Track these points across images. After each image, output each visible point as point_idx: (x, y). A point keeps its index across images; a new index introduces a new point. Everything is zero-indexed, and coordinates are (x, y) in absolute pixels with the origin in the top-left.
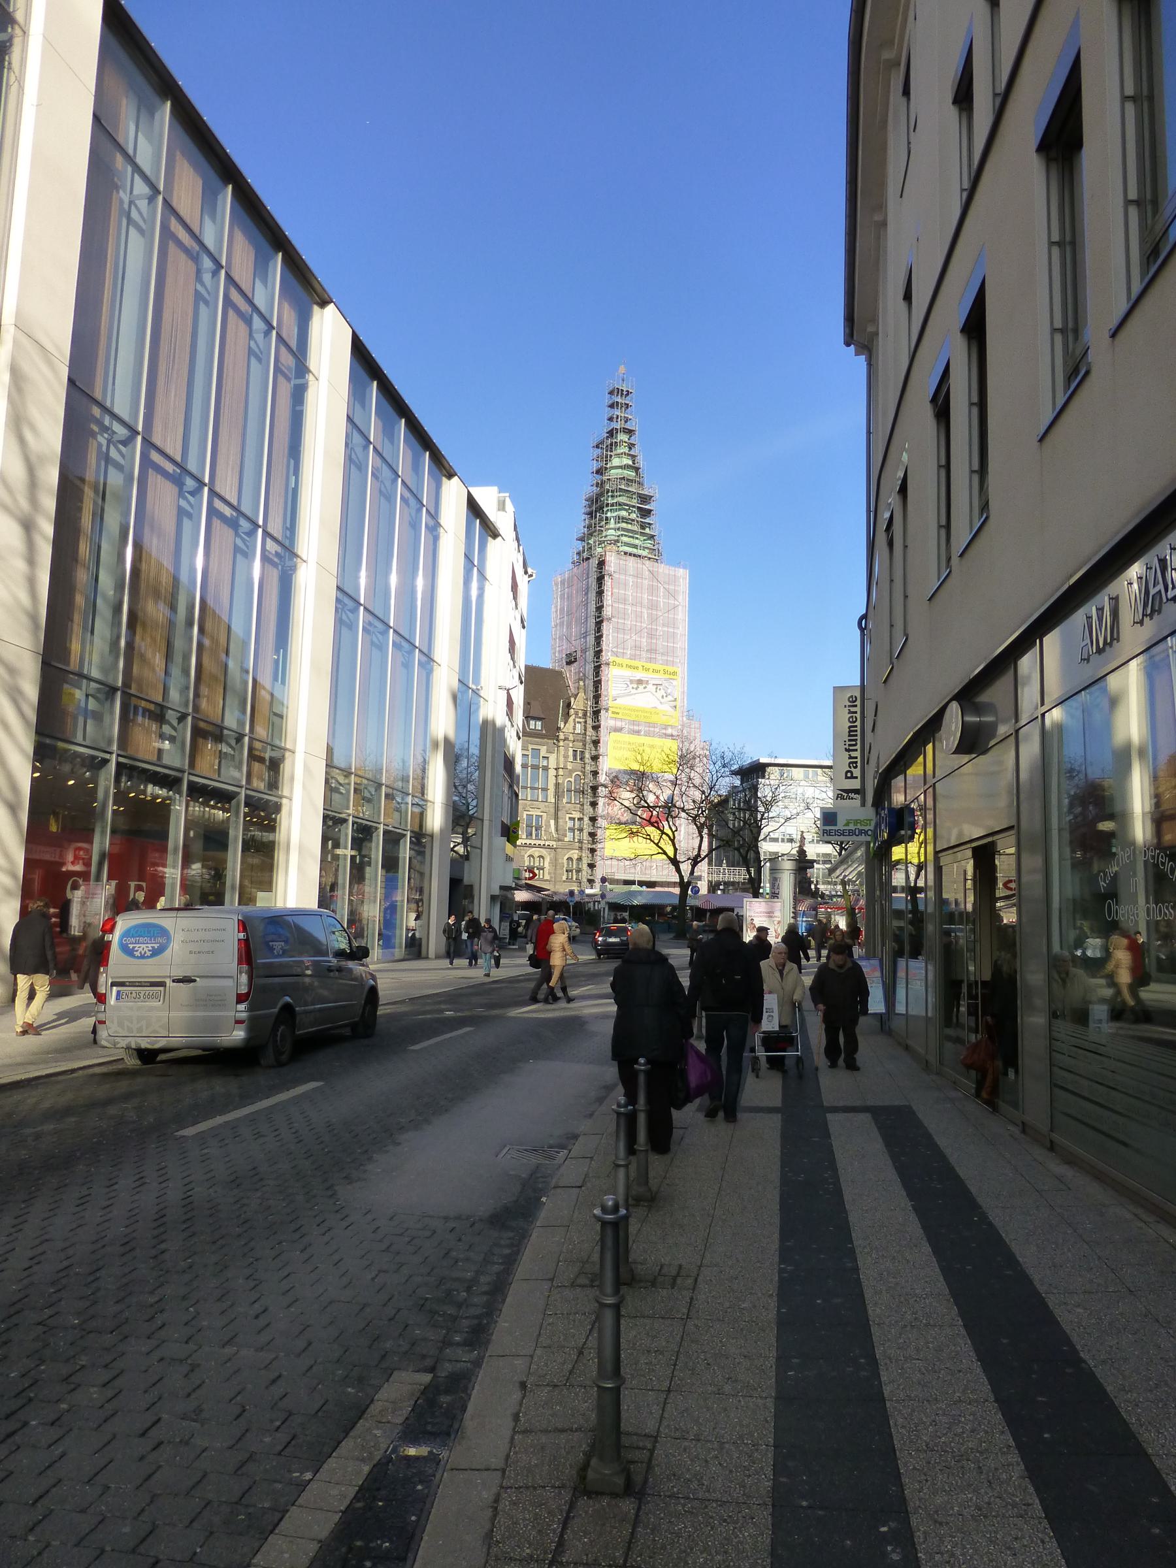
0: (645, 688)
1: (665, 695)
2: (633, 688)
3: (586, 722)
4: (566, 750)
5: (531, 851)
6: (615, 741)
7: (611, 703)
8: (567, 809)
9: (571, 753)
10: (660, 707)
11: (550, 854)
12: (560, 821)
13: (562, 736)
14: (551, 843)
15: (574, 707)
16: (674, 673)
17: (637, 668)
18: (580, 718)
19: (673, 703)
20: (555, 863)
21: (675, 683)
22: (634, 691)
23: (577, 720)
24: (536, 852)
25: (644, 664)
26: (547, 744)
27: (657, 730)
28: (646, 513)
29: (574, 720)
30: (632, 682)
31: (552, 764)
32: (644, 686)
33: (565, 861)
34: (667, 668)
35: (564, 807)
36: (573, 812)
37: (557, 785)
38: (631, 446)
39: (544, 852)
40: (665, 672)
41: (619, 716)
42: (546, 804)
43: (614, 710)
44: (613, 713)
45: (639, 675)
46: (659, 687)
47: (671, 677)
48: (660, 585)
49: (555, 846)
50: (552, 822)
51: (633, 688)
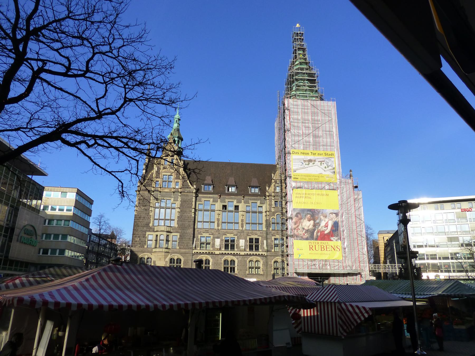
0: (313, 164)
1: (327, 166)
2: (306, 164)
3: (282, 186)
4: (271, 201)
5: (251, 258)
6: (297, 194)
7: (293, 174)
8: (272, 233)
9: (273, 202)
10: (324, 173)
11: (263, 259)
12: (269, 241)
13: (267, 194)
14: (263, 253)
15: (274, 178)
16: (332, 154)
17: (308, 154)
18: (278, 184)
19: (333, 170)
20: (266, 264)
21: (332, 159)
22: (307, 166)
23: (276, 185)
24: (254, 258)
25: (312, 151)
26: (260, 200)
27: (323, 185)
28: (313, 81)
29: (275, 185)
30: (305, 161)
31: (264, 209)
32: (313, 162)
33: (273, 263)
34: (326, 152)
35: (271, 232)
36: (276, 235)
37: (267, 221)
38: (304, 55)
39: (259, 258)
40: (326, 154)
41: (299, 180)
42: (261, 231)
43: (295, 177)
44: (294, 178)
45: (310, 157)
46: (322, 163)
47: (330, 156)
48: (318, 111)
49: (266, 255)
50: (265, 242)
51: (306, 164)
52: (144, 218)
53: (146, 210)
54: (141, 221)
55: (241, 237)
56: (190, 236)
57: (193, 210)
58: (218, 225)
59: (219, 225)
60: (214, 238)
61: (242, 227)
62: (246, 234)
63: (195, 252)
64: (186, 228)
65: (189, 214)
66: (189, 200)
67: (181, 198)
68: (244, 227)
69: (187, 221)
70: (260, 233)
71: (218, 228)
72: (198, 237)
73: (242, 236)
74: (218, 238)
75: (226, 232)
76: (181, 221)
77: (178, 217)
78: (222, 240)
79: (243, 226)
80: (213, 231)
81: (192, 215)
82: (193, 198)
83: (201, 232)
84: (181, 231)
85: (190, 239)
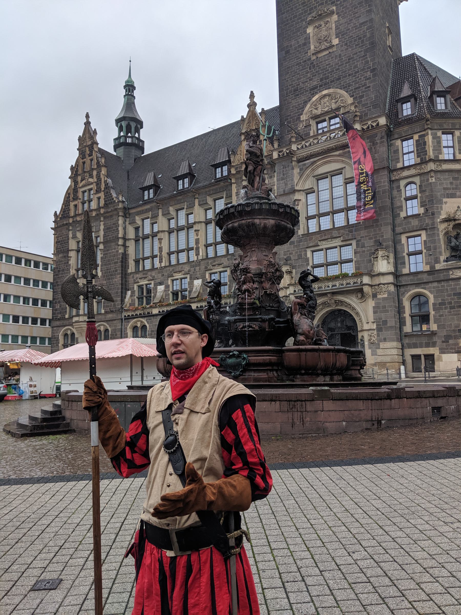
52: (63, 270)
53: (65, 257)
54: (61, 277)
55: (196, 275)
56: (118, 289)
57: (121, 242)
58: (161, 262)
59: (162, 259)
60: (156, 285)
61: (197, 254)
62: (204, 267)
63: (125, 316)
64: (111, 275)
65: (115, 249)
66: (114, 224)
67: (104, 224)
68: (201, 254)
69: (112, 264)
70: (228, 259)
71: (161, 265)
72: (133, 288)
73: (198, 273)
74: (161, 284)
75: (173, 270)
76: (105, 265)
77: (102, 258)
78: (167, 287)
79: (199, 252)
80: (153, 273)
81: (117, 251)
82: (118, 220)
83: (137, 278)
84: (105, 282)
85: (117, 293)
